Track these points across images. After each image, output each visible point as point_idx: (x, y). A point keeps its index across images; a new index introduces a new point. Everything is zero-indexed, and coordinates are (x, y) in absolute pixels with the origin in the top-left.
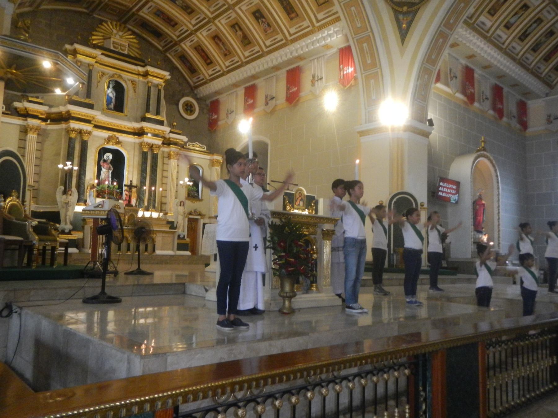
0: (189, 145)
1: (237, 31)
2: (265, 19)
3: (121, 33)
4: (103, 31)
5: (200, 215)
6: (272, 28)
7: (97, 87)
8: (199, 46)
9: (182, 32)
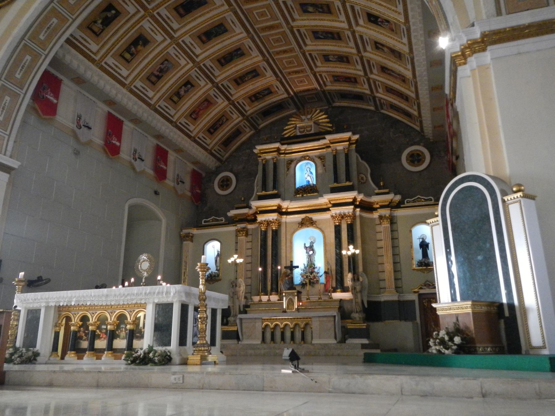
0: (407, 203)
1: (383, 50)
3: (309, 116)
4: (293, 122)
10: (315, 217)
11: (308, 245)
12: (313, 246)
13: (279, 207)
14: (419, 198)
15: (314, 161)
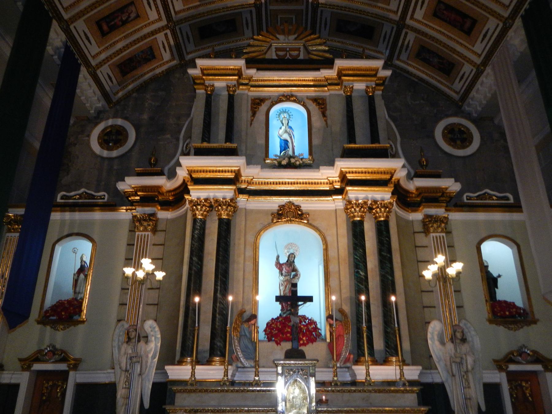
0: (467, 199)
5: (537, 358)
7: (251, 124)
11: (283, 260)
12: (294, 262)
13: (238, 174)
14: (486, 193)
15: (304, 106)
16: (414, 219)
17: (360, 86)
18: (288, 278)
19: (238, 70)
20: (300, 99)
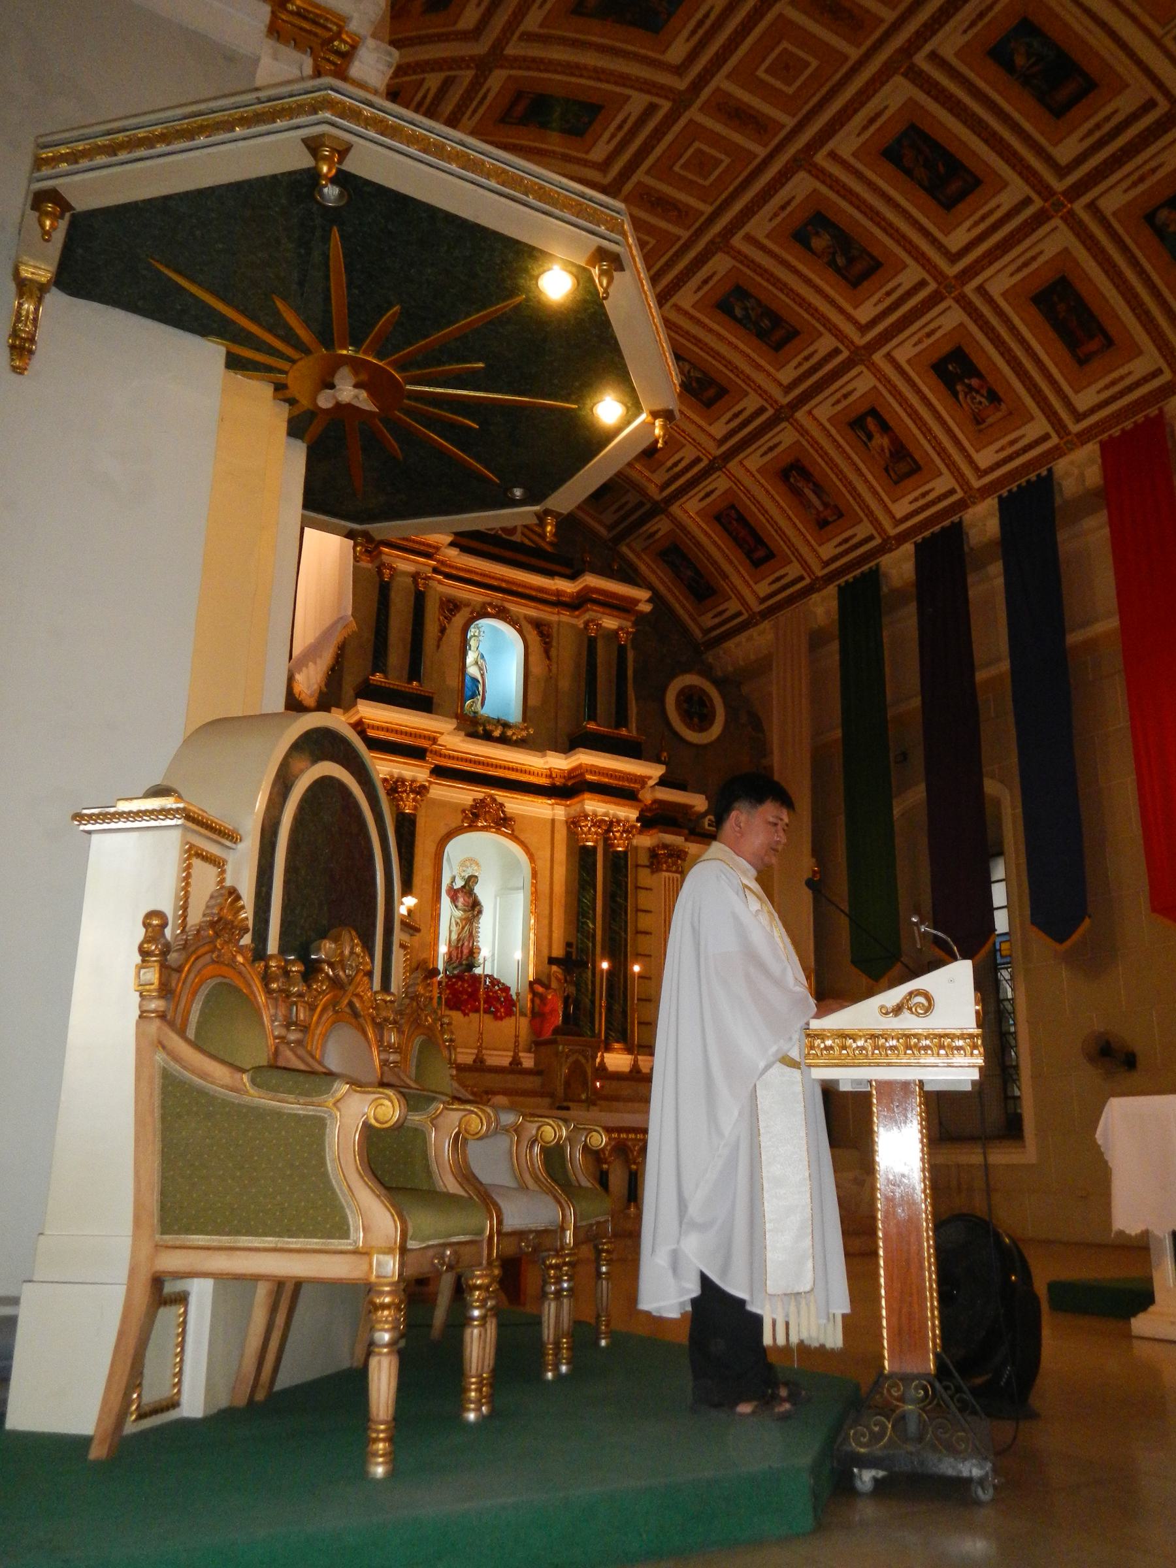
1: (870, 437)
2: (978, 374)
6: (1003, 406)
7: (438, 646)
8: (733, 507)
9: (677, 469)
10: (516, 804)
11: (459, 884)
15: (520, 632)
16: (639, 844)
17: (610, 623)
18: (469, 914)
19: (434, 547)
20: (515, 618)
